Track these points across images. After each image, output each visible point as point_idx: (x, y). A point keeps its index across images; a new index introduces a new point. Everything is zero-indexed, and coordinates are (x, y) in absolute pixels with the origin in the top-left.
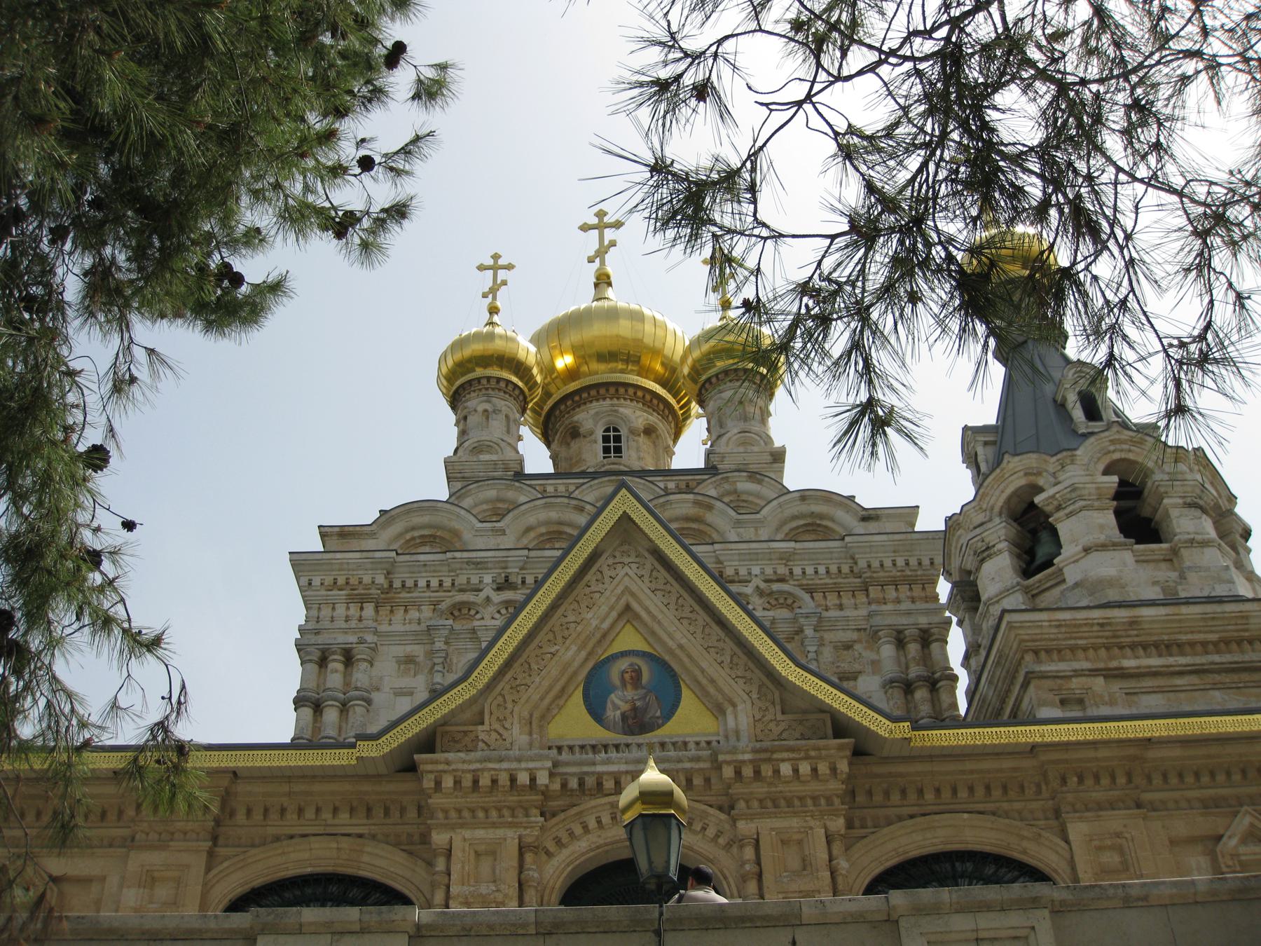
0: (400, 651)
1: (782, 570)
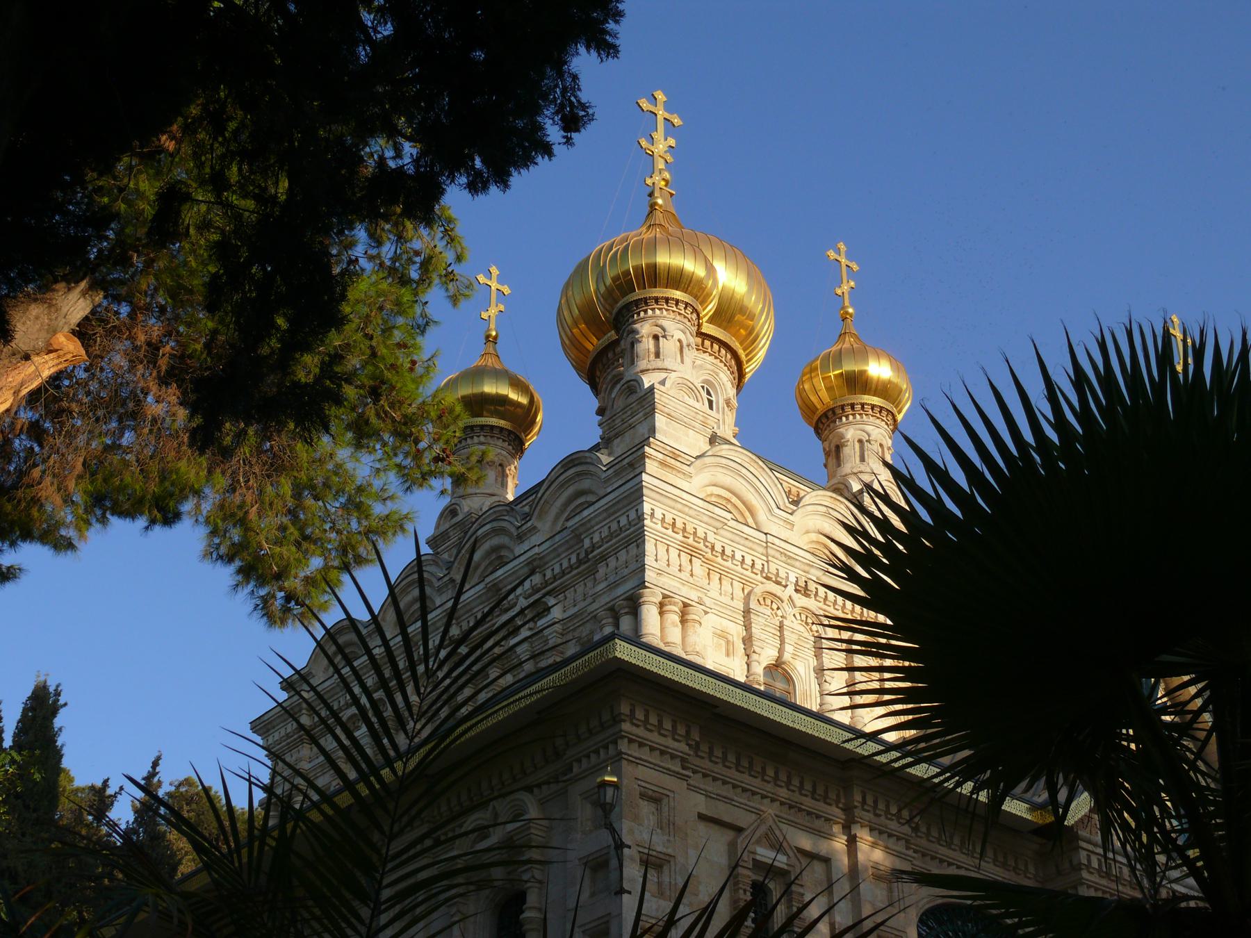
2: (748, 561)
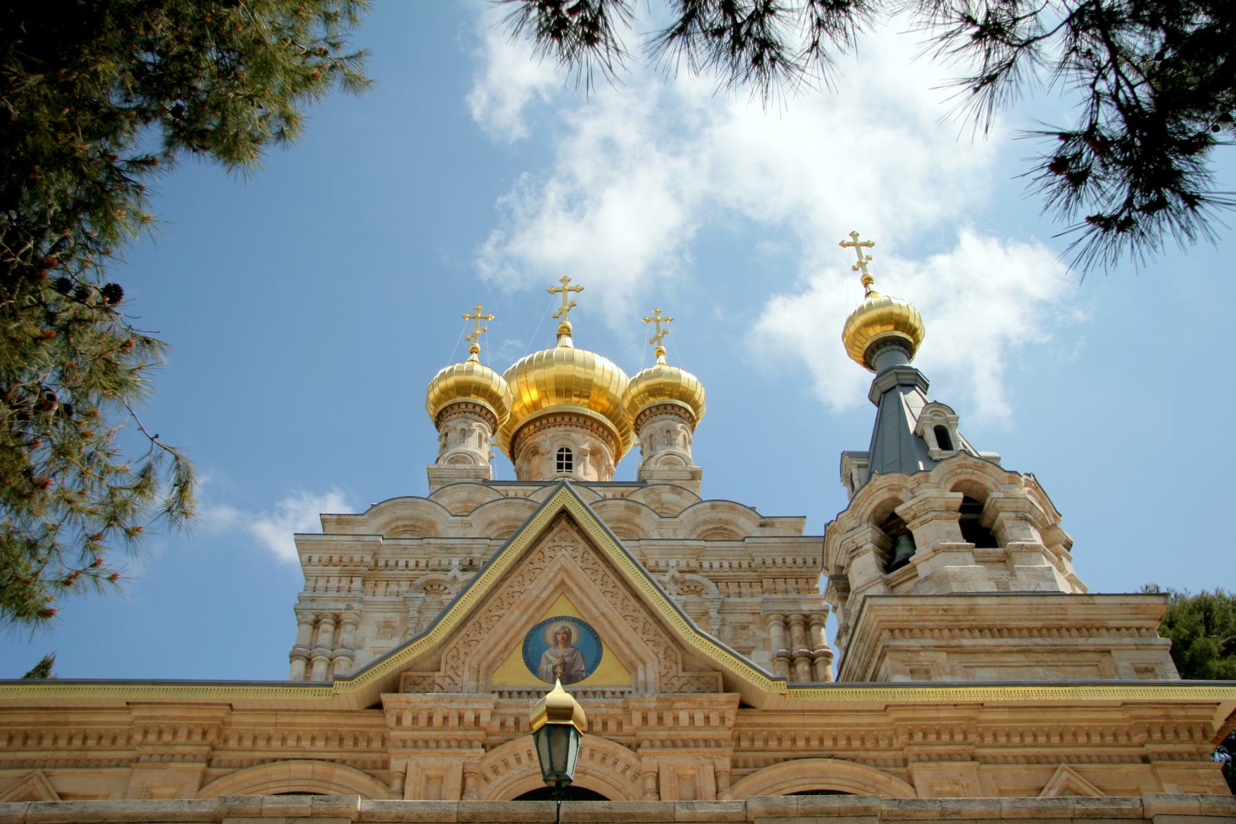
0: (380, 617)
1: (694, 564)
2: (412, 564)
